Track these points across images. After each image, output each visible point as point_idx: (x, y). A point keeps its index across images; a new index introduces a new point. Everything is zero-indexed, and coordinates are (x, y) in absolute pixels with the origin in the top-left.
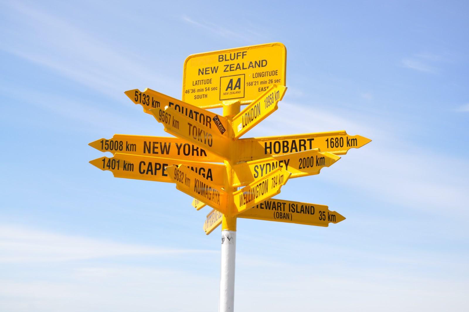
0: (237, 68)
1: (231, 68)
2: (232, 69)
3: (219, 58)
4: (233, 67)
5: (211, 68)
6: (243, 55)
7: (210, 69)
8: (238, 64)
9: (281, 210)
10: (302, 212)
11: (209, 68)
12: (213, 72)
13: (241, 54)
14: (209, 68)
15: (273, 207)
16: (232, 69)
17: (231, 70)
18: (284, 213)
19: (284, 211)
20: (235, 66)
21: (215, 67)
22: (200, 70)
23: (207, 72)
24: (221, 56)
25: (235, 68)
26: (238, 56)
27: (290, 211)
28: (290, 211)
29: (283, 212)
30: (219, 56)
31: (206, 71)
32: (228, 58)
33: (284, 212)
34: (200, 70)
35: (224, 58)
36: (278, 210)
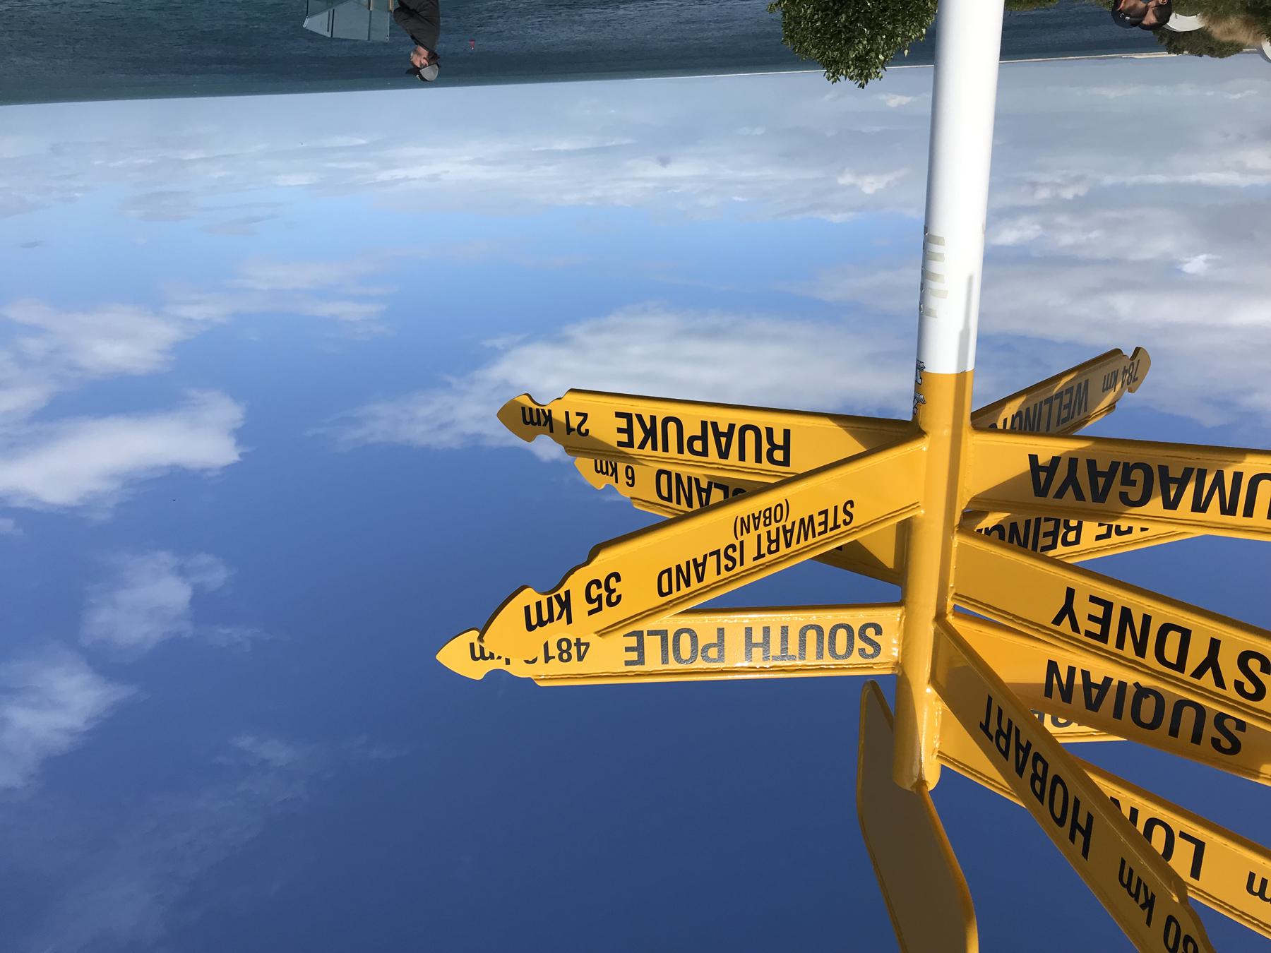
9: (769, 533)
10: (700, 561)
15: (791, 531)
18: (756, 528)
19: (759, 536)
27: (742, 543)
28: (742, 543)
29: (763, 530)
33: (758, 532)
36: (778, 529)
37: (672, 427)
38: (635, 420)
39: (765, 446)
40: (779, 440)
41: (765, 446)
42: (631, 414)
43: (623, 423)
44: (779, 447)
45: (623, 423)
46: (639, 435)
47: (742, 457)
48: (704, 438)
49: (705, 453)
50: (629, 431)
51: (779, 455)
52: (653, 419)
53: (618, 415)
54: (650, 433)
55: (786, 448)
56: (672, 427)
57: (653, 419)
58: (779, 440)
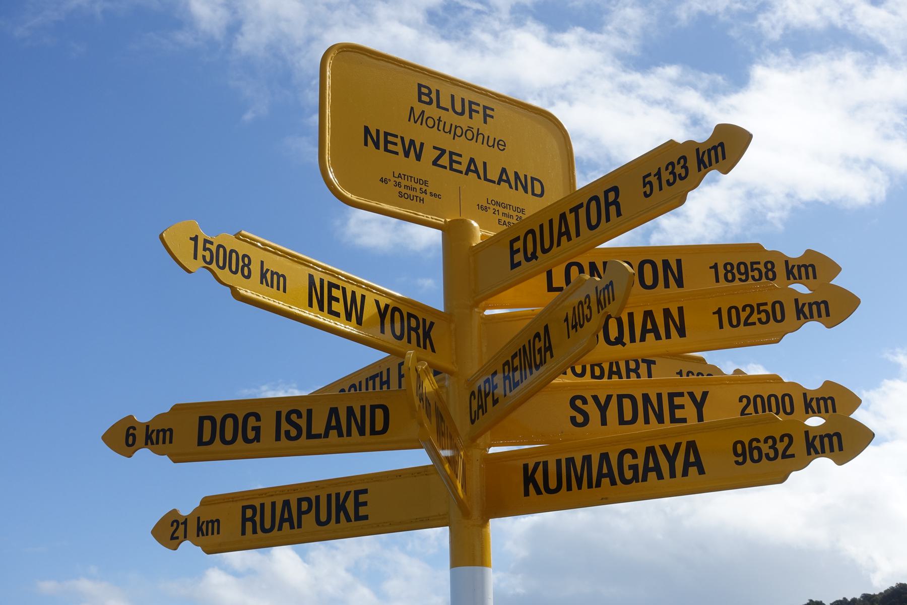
0: (468, 170)
1: (452, 161)
2: (455, 166)
3: (420, 94)
4: (460, 163)
5: (402, 138)
6: (486, 116)
7: (398, 141)
8: (472, 160)
11: (396, 136)
12: (407, 155)
13: (481, 109)
14: (396, 136)
16: (455, 166)
17: (451, 169)
20: (465, 161)
21: (412, 142)
22: (367, 130)
23: (390, 147)
24: (425, 87)
25: (463, 168)
26: (471, 110)
30: (420, 86)
31: (387, 142)
32: (445, 102)
34: (367, 130)
35: (434, 96)
37: (323, 518)
38: (353, 519)
39: (258, 519)
40: (249, 525)
41: (258, 519)
42: (355, 521)
43: (362, 511)
44: (249, 519)
45: (362, 511)
46: (350, 505)
47: (273, 504)
48: (300, 513)
49: (300, 501)
50: (358, 505)
51: (249, 513)
52: (338, 521)
53: (366, 517)
54: (341, 507)
55: (244, 520)
56: (323, 518)
57: (338, 521)
58: (249, 525)
